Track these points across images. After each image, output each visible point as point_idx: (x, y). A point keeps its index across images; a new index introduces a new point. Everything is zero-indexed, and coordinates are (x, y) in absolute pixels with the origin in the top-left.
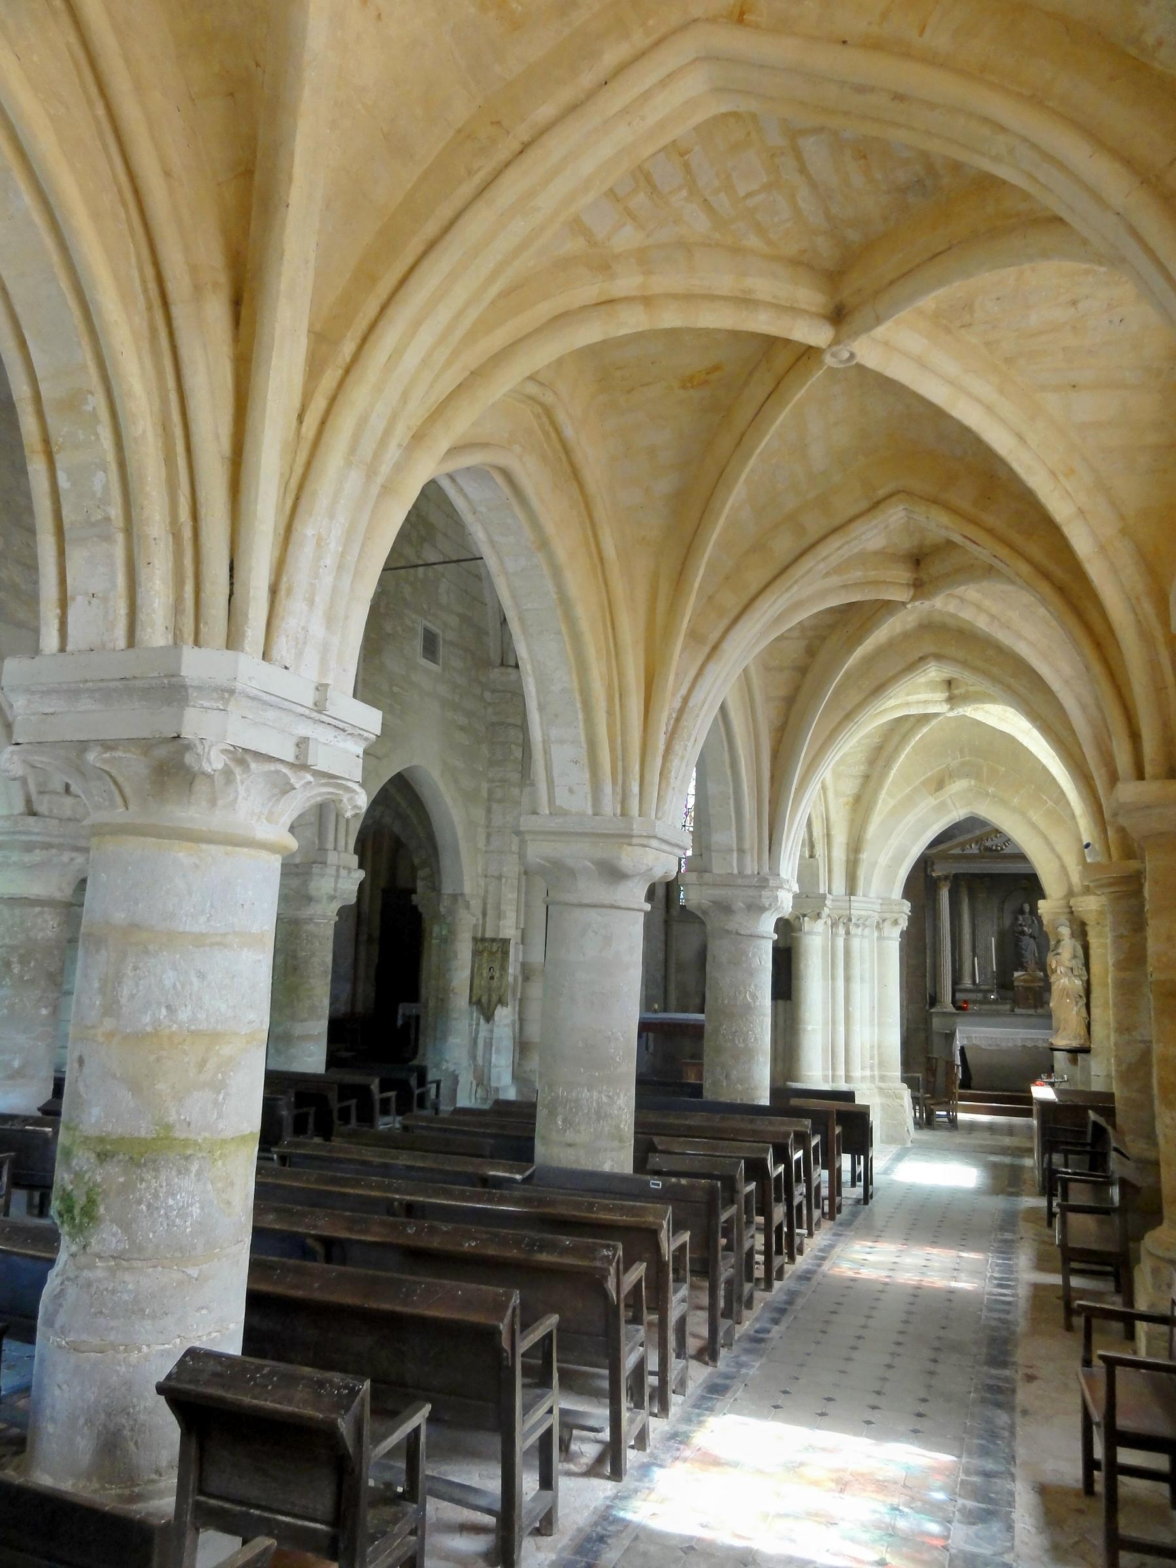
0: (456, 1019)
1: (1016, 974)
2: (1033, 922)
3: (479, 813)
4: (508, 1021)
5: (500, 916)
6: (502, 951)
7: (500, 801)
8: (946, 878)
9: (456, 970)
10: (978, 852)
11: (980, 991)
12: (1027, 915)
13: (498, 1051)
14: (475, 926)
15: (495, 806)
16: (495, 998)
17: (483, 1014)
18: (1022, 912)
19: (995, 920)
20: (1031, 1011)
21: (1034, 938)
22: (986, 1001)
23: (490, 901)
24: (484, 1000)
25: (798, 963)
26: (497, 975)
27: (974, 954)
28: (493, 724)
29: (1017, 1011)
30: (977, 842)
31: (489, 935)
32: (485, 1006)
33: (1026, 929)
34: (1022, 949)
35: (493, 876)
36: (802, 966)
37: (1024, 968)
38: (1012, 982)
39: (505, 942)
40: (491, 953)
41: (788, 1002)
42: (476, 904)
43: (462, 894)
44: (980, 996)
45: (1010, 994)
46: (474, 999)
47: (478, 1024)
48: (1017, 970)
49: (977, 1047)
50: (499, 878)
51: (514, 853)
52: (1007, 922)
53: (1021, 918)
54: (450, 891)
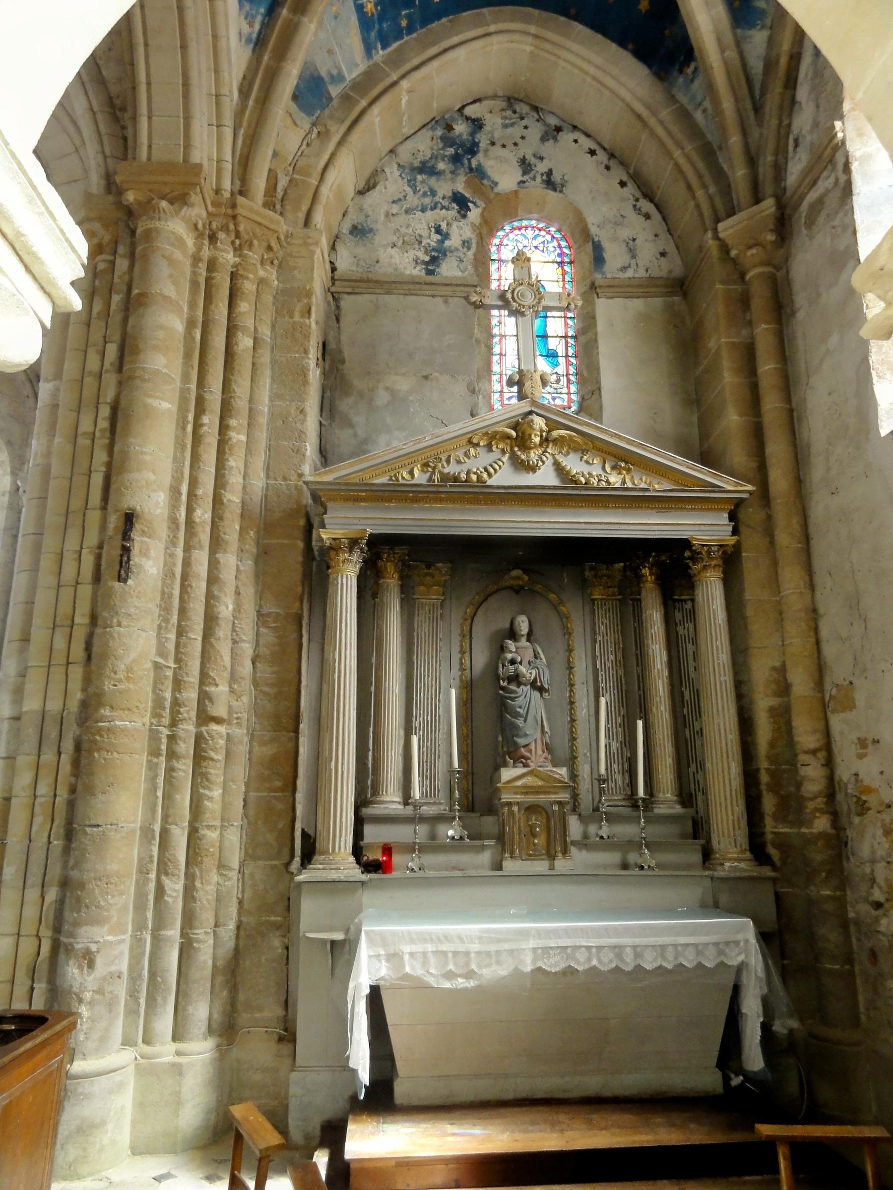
1: (507, 774)
2: (536, 656)
8: (353, 543)
10: (424, 482)
11: (422, 819)
12: (523, 642)
18: (512, 634)
19: (456, 657)
20: (541, 866)
21: (541, 690)
22: (433, 845)
27: (408, 730)
29: (509, 865)
30: (426, 465)
33: (523, 669)
34: (517, 715)
37: (519, 759)
38: (496, 792)
44: (422, 830)
45: (489, 823)
48: (505, 765)
49: (419, 987)
52: (480, 658)
53: (511, 645)
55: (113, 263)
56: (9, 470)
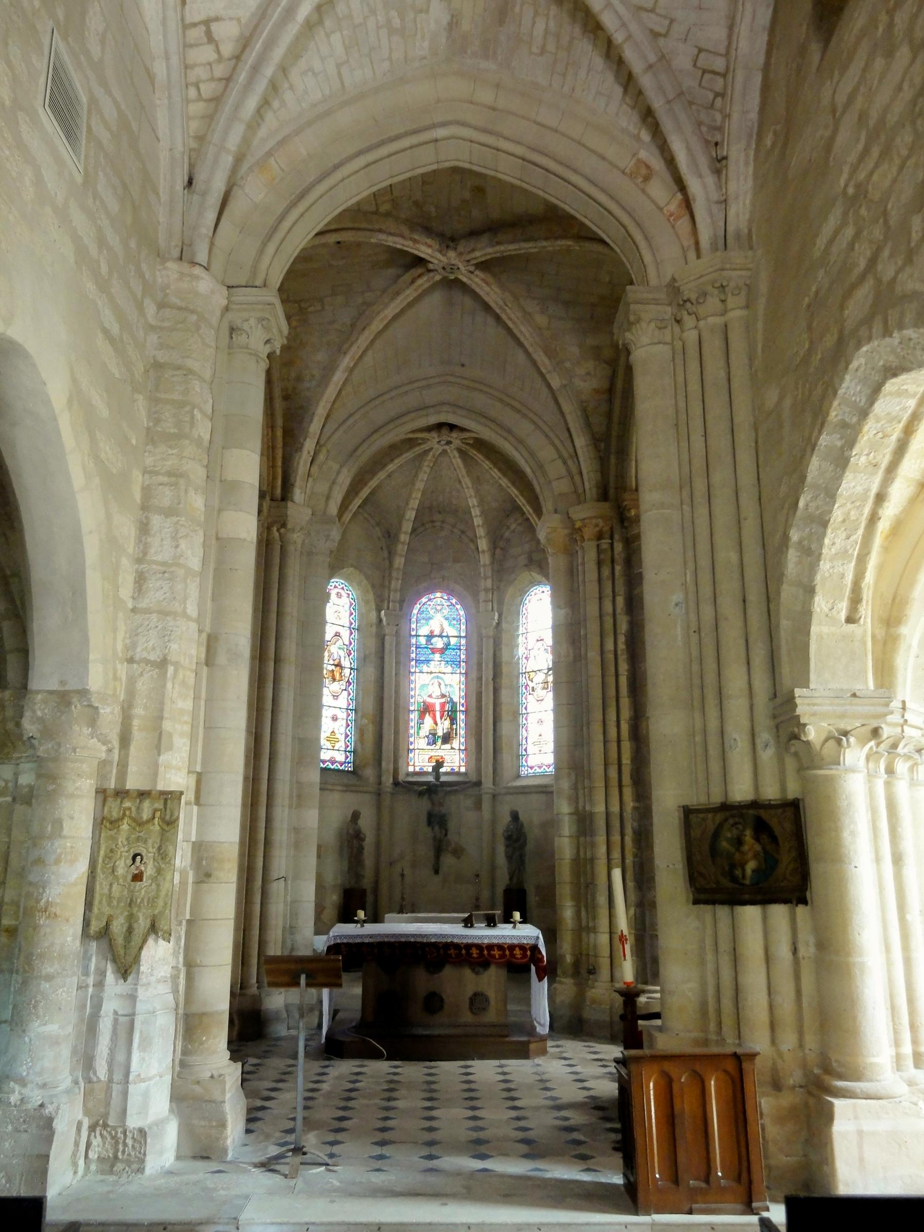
0: (49, 978)
3: (126, 528)
4: (165, 971)
5: (159, 742)
6: (162, 819)
7: (169, 512)
9: (58, 861)
13: (146, 1043)
14: (104, 764)
15: (156, 520)
16: (142, 924)
17: (114, 961)
23: (138, 711)
24: (118, 927)
25: (837, 830)
26: (149, 871)
28: (158, 366)
31: (133, 783)
32: (120, 941)
35: (147, 662)
36: (846, 834)
39: (170, 798)
40: (139, 823)
41: (800, 910)
42: (109, 714)
43: (83, 693)
46: (95, 926)
47: (100, 985)
50: (162, 664)
51: (189, 618)
54: (54, 685)
55: (612, 545)
56: (374, 607)
